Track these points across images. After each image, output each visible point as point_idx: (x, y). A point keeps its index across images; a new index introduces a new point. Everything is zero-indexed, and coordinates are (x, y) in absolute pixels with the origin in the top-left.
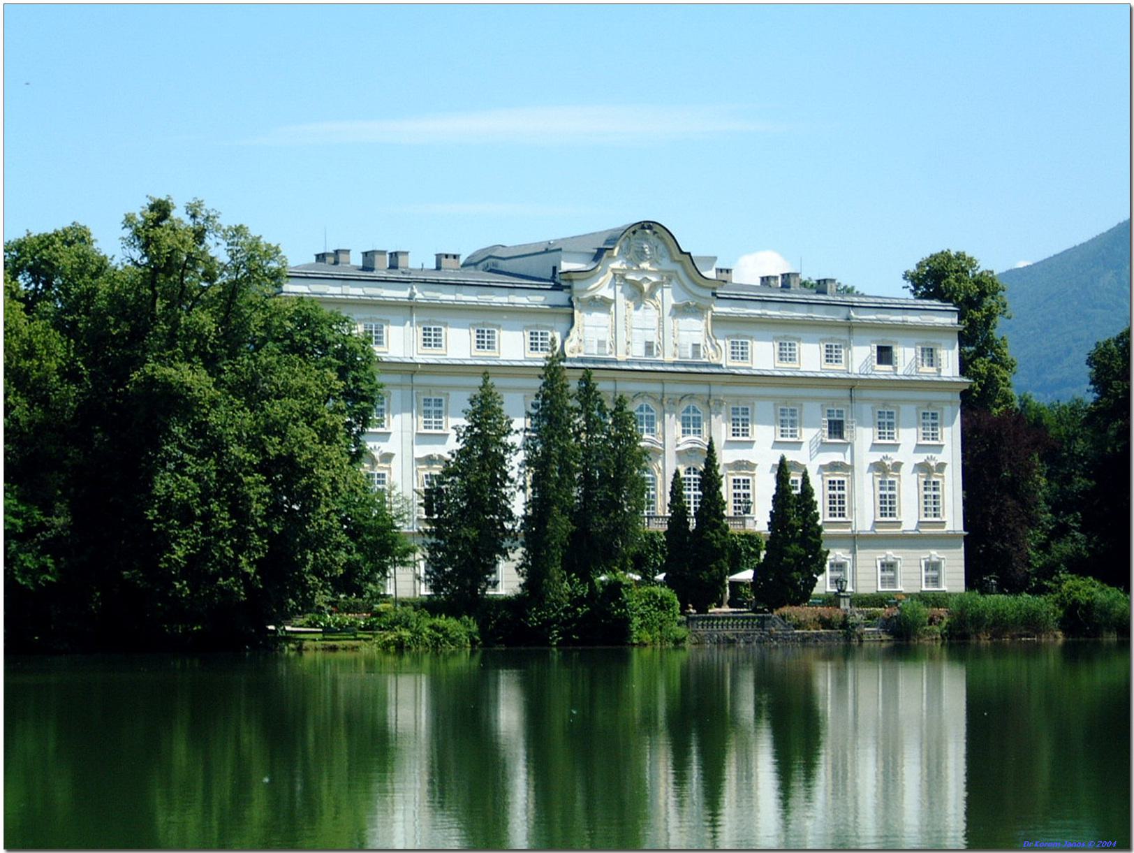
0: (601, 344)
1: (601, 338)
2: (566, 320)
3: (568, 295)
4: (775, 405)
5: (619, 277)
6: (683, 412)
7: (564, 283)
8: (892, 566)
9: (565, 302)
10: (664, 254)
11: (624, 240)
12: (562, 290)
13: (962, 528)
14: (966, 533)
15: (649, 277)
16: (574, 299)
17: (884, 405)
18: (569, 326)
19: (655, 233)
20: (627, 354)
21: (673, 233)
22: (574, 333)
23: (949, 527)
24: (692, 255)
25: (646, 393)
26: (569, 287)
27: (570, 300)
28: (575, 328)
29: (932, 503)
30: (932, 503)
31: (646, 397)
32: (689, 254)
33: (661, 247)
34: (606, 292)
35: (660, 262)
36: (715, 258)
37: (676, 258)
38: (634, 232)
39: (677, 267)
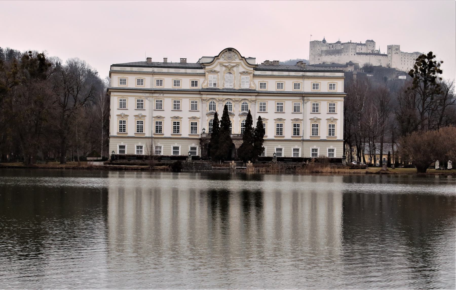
0: (215, 84)
5: (222, 65)
6: (242, 104)
7: (203, 67)
12: (202, 69)
13: (343, 139)
19: (233, 51)
23: (339, 138)
25: (229, 99)
29: (331, 131)
30: (331, 131)
31: (229, 100)
32: (244, 57)
33: (236, 56)
34: (218, 69)
38: (226, 51)
39: (241, 61)
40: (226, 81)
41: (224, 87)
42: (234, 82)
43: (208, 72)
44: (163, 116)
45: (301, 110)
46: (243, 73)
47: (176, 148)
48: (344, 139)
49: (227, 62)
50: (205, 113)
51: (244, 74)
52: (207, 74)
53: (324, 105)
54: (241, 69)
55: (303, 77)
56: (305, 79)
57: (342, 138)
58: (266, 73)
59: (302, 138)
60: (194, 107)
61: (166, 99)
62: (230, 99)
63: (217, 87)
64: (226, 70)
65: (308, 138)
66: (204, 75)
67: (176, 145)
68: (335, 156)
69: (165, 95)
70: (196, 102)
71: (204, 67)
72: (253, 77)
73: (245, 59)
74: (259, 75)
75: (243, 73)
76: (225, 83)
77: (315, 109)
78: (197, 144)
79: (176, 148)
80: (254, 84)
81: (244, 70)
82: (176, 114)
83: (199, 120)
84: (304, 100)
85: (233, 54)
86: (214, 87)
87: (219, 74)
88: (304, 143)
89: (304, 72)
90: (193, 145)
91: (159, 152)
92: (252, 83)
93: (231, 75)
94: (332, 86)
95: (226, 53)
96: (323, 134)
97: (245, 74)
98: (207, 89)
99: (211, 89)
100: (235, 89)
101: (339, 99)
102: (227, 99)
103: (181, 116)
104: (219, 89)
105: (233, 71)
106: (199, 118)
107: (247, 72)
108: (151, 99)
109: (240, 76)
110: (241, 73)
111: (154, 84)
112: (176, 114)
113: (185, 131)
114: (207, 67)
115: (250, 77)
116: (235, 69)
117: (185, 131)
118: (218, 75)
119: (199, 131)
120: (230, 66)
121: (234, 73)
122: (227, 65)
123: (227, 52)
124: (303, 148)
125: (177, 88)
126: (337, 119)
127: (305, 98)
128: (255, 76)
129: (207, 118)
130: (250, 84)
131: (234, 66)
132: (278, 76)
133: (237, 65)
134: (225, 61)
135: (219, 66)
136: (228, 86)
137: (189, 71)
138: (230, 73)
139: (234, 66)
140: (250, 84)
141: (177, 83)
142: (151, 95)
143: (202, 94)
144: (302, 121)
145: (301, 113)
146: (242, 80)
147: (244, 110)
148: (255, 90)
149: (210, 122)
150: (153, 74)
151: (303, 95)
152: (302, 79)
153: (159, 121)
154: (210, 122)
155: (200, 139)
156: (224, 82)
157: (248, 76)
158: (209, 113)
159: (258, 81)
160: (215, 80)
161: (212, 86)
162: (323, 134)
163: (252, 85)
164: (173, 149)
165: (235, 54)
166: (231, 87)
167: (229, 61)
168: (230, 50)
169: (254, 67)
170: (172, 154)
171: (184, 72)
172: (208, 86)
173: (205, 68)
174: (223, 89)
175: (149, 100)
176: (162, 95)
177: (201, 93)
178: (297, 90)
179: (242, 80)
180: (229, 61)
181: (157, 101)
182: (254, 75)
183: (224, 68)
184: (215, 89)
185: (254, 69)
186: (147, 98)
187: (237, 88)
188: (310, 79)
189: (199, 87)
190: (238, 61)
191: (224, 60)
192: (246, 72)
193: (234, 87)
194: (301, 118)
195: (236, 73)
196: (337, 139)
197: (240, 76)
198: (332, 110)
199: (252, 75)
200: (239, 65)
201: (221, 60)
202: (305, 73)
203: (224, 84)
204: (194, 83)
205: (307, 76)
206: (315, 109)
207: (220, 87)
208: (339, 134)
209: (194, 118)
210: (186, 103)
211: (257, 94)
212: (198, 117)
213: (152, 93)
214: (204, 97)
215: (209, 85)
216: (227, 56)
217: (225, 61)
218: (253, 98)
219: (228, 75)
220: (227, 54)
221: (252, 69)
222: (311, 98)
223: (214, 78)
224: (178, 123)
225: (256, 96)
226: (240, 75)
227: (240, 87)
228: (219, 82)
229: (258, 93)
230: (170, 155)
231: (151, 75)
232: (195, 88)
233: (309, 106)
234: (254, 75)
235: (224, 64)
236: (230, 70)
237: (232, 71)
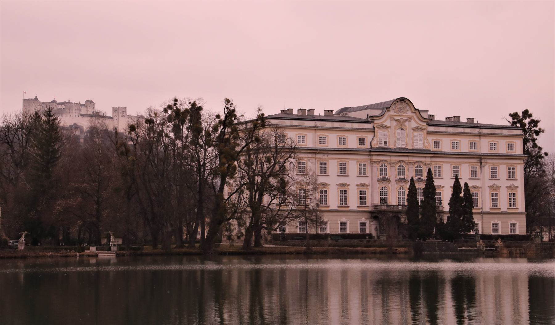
1: (385, 140)
2: (373, 134)
3: (373, 125)
4: (451, 165)
5: (392, 118)
6: (416, 167)
8: (514, 225)
9: (372, 128)
10: (409, 110)
11: (393, 105)
12: (370, 123)
14: (527, 213)
15: (403, 118)
16: (375, 126)
17: (493, 165)
18: (373, 136)
19: (405, 102)
20: (395, 146)
21: (412, 103)
22: (375, 139)
23: (520, 210)
24: (419, 110)
26: (373, 122)
27: (373, 127)
28: (375, 137)
29: (512, 201)
30: (512, 201)
31: (402, 162)
32: (418, 109)
33: (408, 108)
34: (388, 123)
35: (407, 112)
36: (427, 111)
37: (413, 111)
38: (397, 102)
39: (414, 115)
40: (399, 139)
41: (395, 146)
42: (406, 140)
43: (377, 127)
44: (328, 183)
45: (479, 176)
46: (417, 129)
47: (343, 224)
48: (526, 211)
49: (398, 114)
50: (375, 179)
51: (417, 130)
52: (376, 129)
53: (503, 170)
54: (414, 124)
55: (480, 135)
56: (482, 137)
57: (524, 210)
58: (440, 129)
59: (480, 211)
60: (362, 172)
61: (350, 162)
62: (403, 161)
63: (388, 146)
64: (397, 125)
65: (488, 210)
66: (373, 131)
67: (344, 220)
68: (518, 233)
69: (330, 156)
70: (364, 165)
71: (373, 121)
72: (427, 134)
73: (419, 111)
74: (433, 132)
75: (417, 129)
76: (396, 141)
77: (494, 175)
78: (367, 219)
79: (343, 224)
80: (428, 143)
81: (417, 126)
82: (343, 180)
83: (368, 187)
84: (481, 163)
85: (405, 105)
86: (385, 147)
87: (389, 129)
88: (484, 216)
89: (481, 128)
90: (363, 220)
91: (324, 229)
92: (425, 141)
93: (403, 131)
94: (510, 146)
95: (397, 104)
96: (504, 206)
97: (418, 130)
98: (378, 148)
99: (382, 148)
100: (408, 149)
101: (518, 162)
102: (399, 161)
103: (348, 183)
104: (390, 149)
105: (405, 126)
106: (368, 186)
107: (420, 128)
108: (314, 161)
109: (413, 133)
110: (413, 129)
111: (317, 141)
112: (343, 180)
113: (353, 203)
114: (376, 122)
115: (423, 134)
116: (407, 124)
117: (353, 203)
118: (389, 131)
119: (369, 203)
120: (402, 121)
121: (406, 129)
122: (398, 118)
123: (399, 103)
124: (482, 222)
125: (342, 147)
126: (517, 187)
127: (483, 161)
128: (429, 133)
129: (378, 185)
130: (424, 143)
131: (405, 121)
132: (470, 133)
133: (409, 119)
134: (395, 114)
135: (389, 120)
136: (400, 145)
137: (356, 126)
138: (402, 129)
139: (405, 121)
140: (424, 143)
141: (342, 140)
142: (314, 156)
143: (372, 155)
144: (480, 189)
145: (479, 179)
146: (416, 138)
147: (418, 175)
148: (429, 150)
149: (382, 190)
150: (316, 129)
151: (481, 157)
152: (478, 137)
153: (363, 190)
154: (382, 190)
155: (371, 212)
156: (395, 140)
157: (421, 133)
158: (381, 179)
159: (431, 139)
160: (385, 137)
161: (383, 145)
162: (504, 206)
163: (426, 144)
164: (340, 225)
165: (406, 105)
166: (403, 146)
167: (400, 114)
168: (402, 100)
169: (427, 122)
170: (339, 232)
171: (350, 127)
172: (377, 145)
173: (373, 122)
174: (395, 149)
175: (312, 163)
176: (326, 156)
177: (372, 153)
178: (473, 151)
179: (416, 138)
180: (400, 114)
181: (321, 164)
182: (428, 132)
183: (395, 123)
184: (387, 149)
185: (427, 124)
186: (309, 159)
187: (410, 147)
188: (487, 137)
189: (367, 146)
190: (409, 114)
191: (395, 112)
192: (419, 128)
193: (406, 146)
194: (479, 186)
195: (408, 129)
196: (519, 211)
197: (413, 133)
198: (511, 176)
199: (425, 132)
200: (411, 119)
201: (392, 113)
202: (482, 129)
203: (395, 142)
204: (361, 141)
205: (484, 134)
206: (494, 175)
207: (391, 146)
208: (521, 205)
209: (363, 185)
210: (353, 166)
211: (433, 156)
212: (367, 184)
213: (316, 153)
214: (375, 158)
215: (379, 143)
216: (398, 108)
217: (395, 114)
218: (428, 160)
219: (399, 131)
220: (399, 105)
221: (425, 124)
222: (489, 161)
223: (384, 135)
224: (345, 192)
225: (431, 157)
226: (412, 131)
227: (413, 146)
228: (390, 139)
229: (434, 153)
230: (337, 233)
231: (314, 131)
232: (362, 147)
233: (487, 170)
234: (428, 132)
235: (395, 118)
236: (401, 125)
237: (404, 126)
